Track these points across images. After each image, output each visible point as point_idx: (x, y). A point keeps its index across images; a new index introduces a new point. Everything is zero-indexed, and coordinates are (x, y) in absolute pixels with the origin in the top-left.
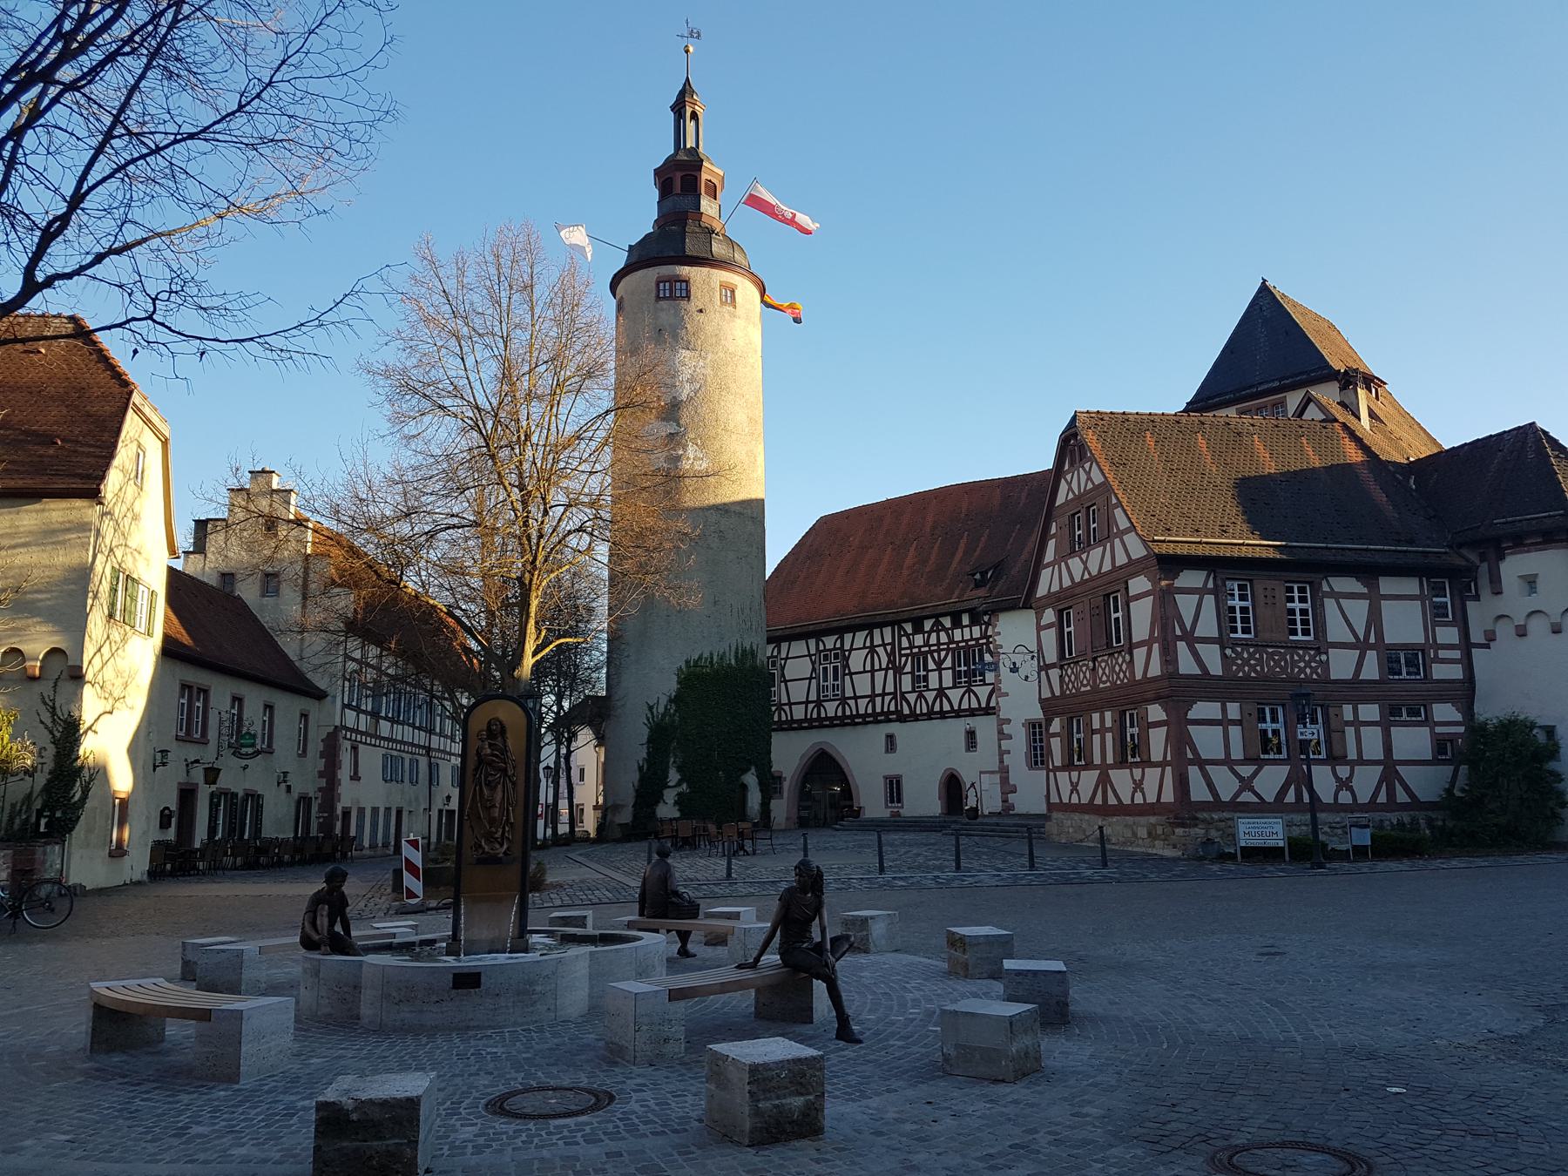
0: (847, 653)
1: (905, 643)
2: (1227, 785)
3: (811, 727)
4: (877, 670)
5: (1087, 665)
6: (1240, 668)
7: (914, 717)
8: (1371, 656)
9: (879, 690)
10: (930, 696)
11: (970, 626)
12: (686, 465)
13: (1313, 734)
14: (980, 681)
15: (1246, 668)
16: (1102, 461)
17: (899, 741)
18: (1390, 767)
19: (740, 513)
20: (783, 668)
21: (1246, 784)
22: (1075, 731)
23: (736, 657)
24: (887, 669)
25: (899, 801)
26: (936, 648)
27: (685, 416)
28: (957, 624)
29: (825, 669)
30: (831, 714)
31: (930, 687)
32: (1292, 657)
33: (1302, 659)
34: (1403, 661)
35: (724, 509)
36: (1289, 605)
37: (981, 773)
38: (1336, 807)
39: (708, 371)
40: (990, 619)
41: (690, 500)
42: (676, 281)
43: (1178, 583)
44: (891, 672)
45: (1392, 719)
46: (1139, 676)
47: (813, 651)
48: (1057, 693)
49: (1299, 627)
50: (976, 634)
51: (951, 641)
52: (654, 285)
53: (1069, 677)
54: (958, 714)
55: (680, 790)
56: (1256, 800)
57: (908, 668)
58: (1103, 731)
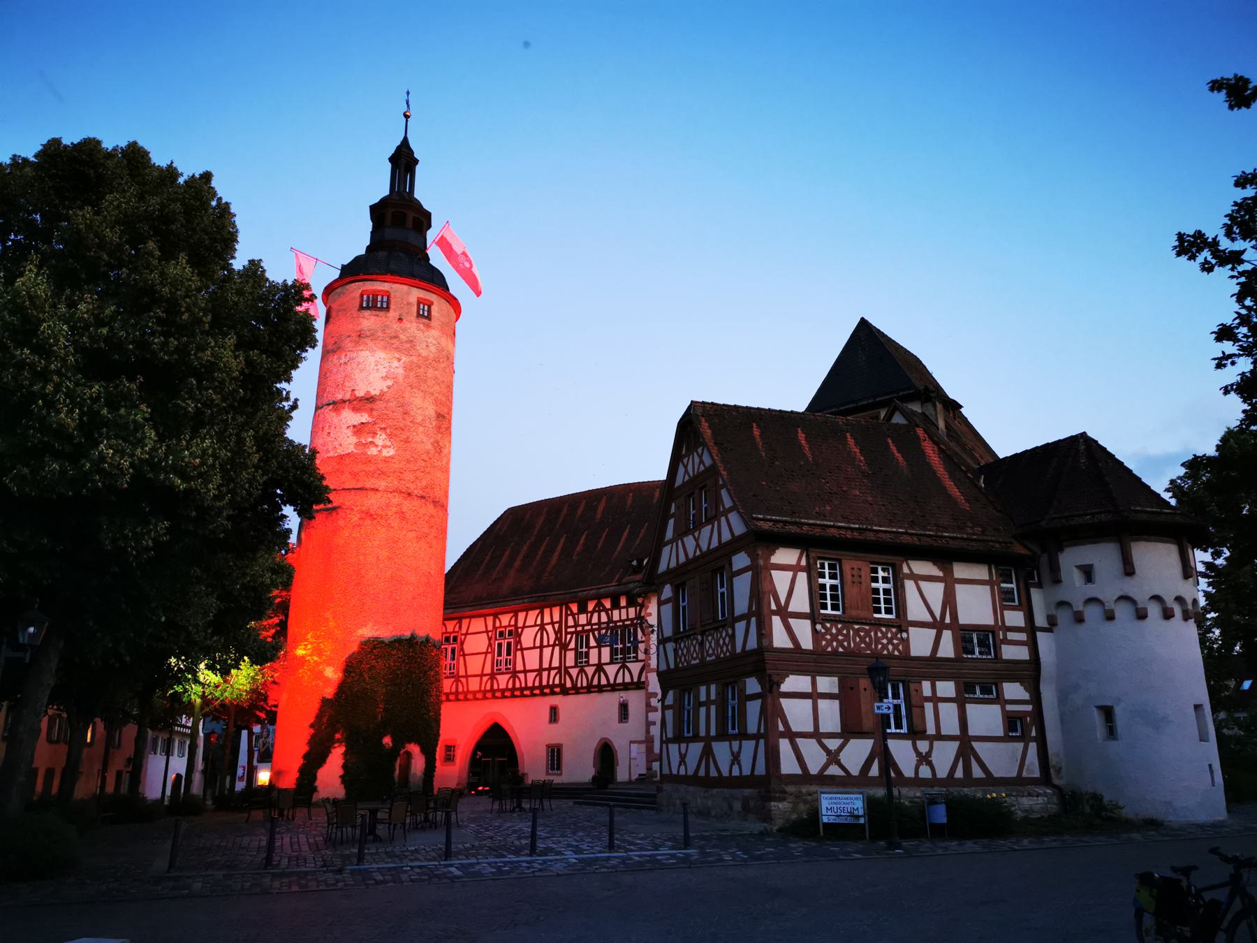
0: (520, 630)
1: (571, 622)
2: (815, 758)
3: (485, 698)
4: (546, 647)
5: (697, 640)
6: (829, 643)
7: (576, 690)
8: (947, 635)
9: (546, 665)
10: (590, 671)
11: (627, 607)
13: (889, 708)
14: (634, 657)
15: (835, 644)
16: (711, 444)
17: (562, 714)
18: (965, 742)
19: (422, 497)
20: (462, 643)
21: (833, 757)
22: (686, 703)
24: (554, 646)
25: (559, 768)
26: (597, 627)
28: (616, 605)
29: (500, 645)
30: (502, 686)
31: (591, 663)
32: (876, 634)
33: (885, 636)
34: (975, 641)
36: (874, 585)
37: (631, 742)
38: (917, 781)
40: (643, 602)
44: (557, 649)
45: (967, 696)
46: (739, 650)
47: (490, 628)
48: (672, 666)
49: (883, 606)
50: (632, 614)
51: (610, 620)
53: (682, 650)
54: (613, 687)
56: (842, 773)
57: (572, 645)
58: (707, 703)
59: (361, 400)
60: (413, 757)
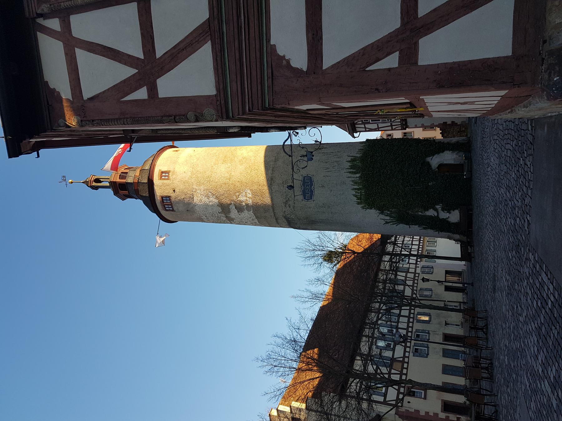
12: (250, 202)
23: (355, 173)
27: (226, 201)
35: (270, 181)
39: (202, 187)
41: (267, 200)
42: (163, 202)
43: (66, 93)
52: (167, 212)
55: (440, 209)
59: (223, 209)
60: (442, 162)
